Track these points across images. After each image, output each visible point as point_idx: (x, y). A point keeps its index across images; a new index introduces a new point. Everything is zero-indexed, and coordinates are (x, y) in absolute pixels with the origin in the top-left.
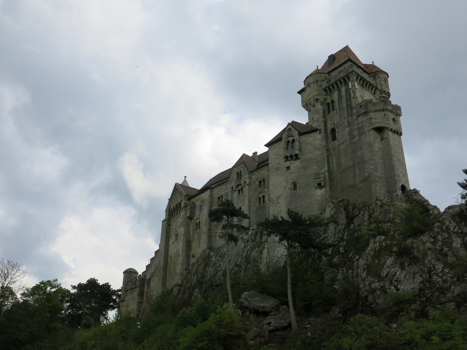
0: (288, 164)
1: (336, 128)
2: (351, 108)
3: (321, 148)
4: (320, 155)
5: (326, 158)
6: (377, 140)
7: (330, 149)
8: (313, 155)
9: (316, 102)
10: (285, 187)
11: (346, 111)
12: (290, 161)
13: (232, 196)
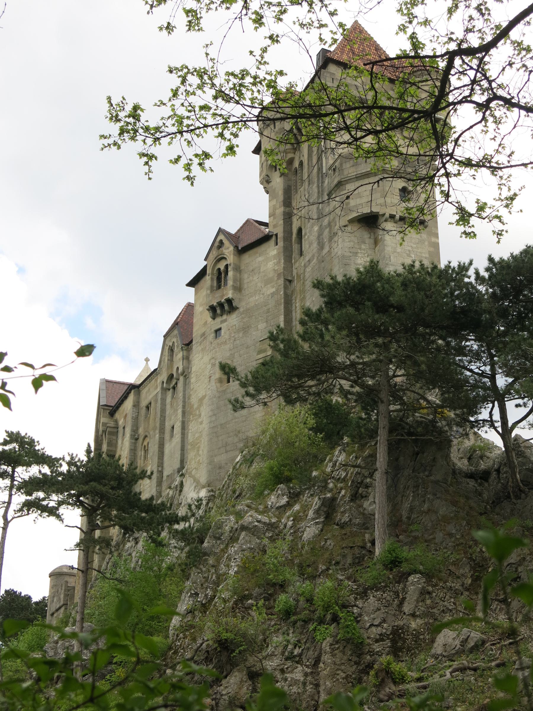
0: (217, 323)
1: (303, 228)
2: (322, 176)
3: (276, 279)
4: (273, 294)
5: (283, 301)
6: (363, 247)
7: (294, 278)
8: (261, 296)
9: (274, 170)
10: (210, 377)
11: (315, 185)
12: (222, 316)
13: (163, 400)
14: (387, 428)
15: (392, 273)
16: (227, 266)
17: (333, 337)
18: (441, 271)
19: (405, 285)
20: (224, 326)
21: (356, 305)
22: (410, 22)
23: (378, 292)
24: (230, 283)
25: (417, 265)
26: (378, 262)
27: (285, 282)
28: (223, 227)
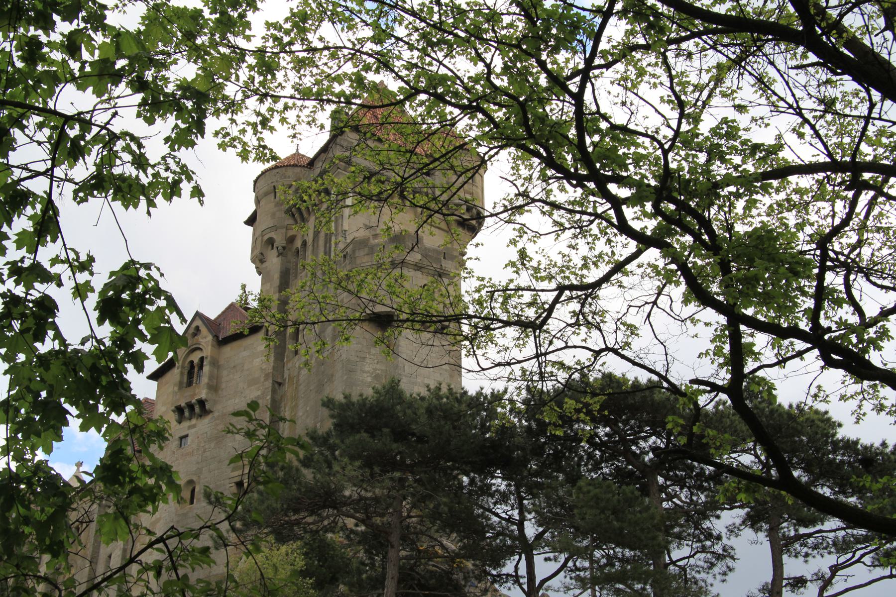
3: (262, 380)
6: (373, 351)
7: (285, 380)
9: (270, 247)
12: (190, 419)
14: (396, 579)
15: (414, 395)
16: (202, 359)
17: (343, 468)
18: (472, 398)
19: (430, 411)
20: (191, 432)
21: (372, 431)
22: (521, 237)
23: (398, 417)
24: (205, 380)
25: (444, 390)
26: (399, 381)
27: (273, 384)
28: (201, 311)
